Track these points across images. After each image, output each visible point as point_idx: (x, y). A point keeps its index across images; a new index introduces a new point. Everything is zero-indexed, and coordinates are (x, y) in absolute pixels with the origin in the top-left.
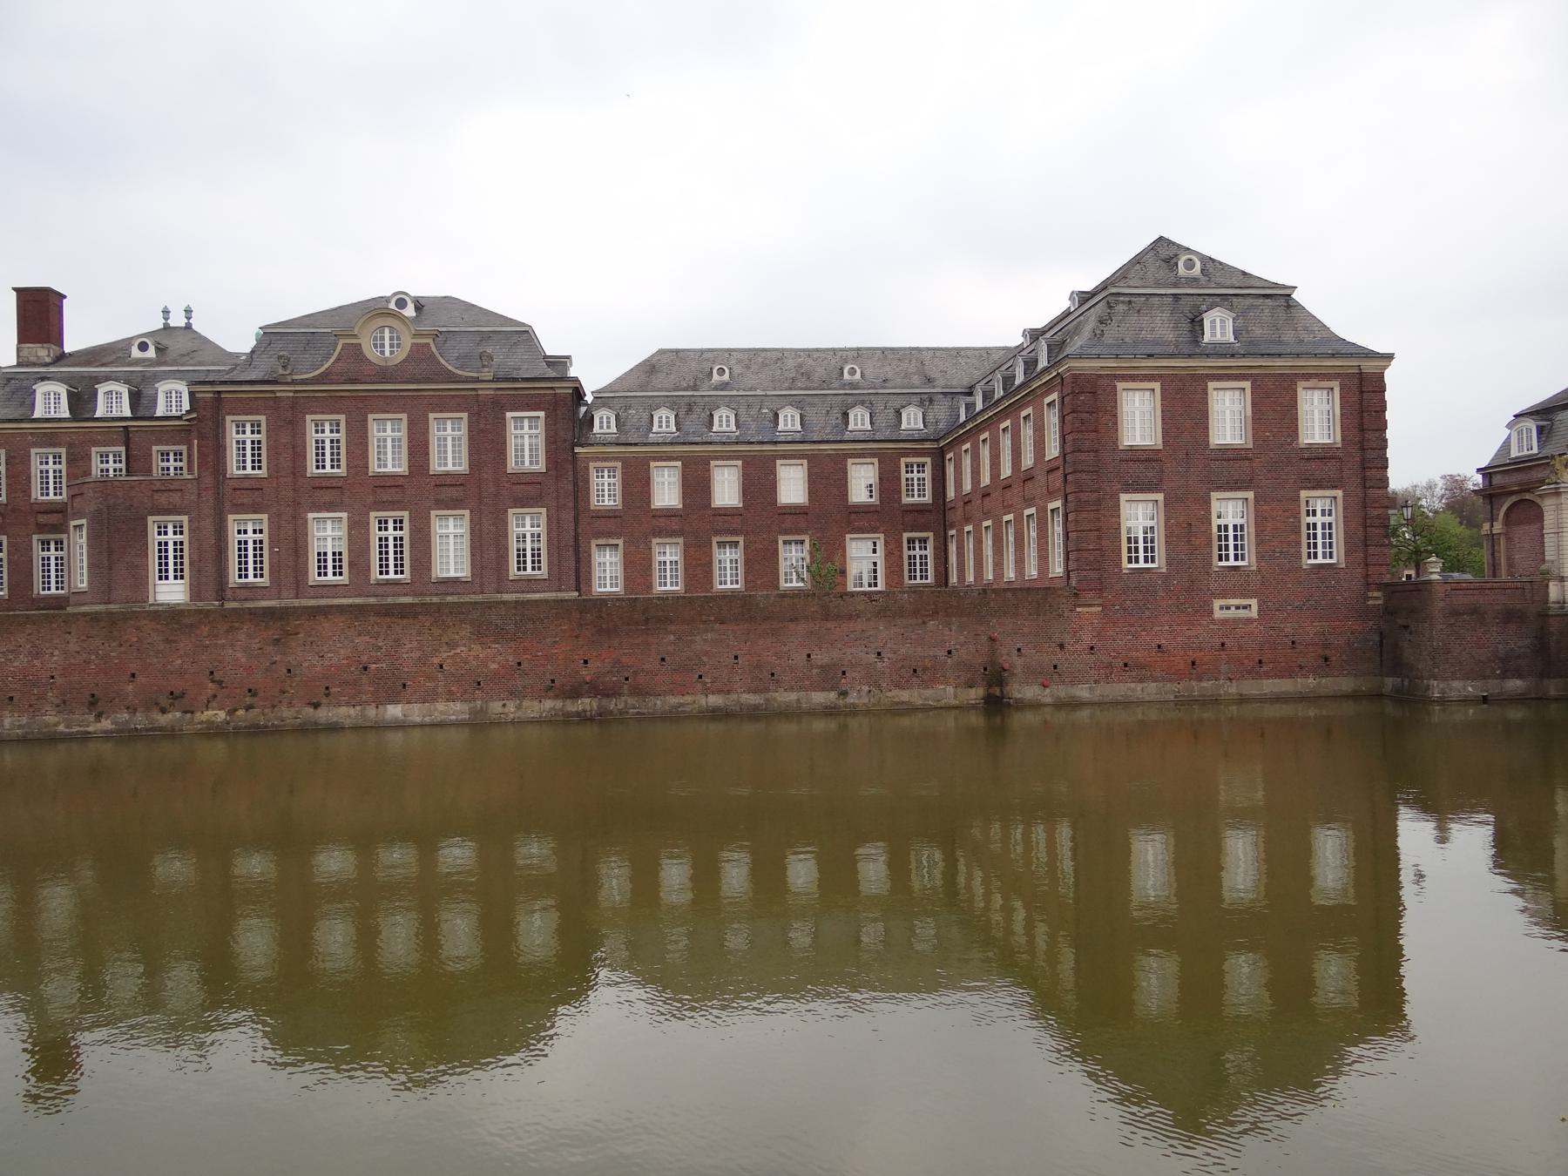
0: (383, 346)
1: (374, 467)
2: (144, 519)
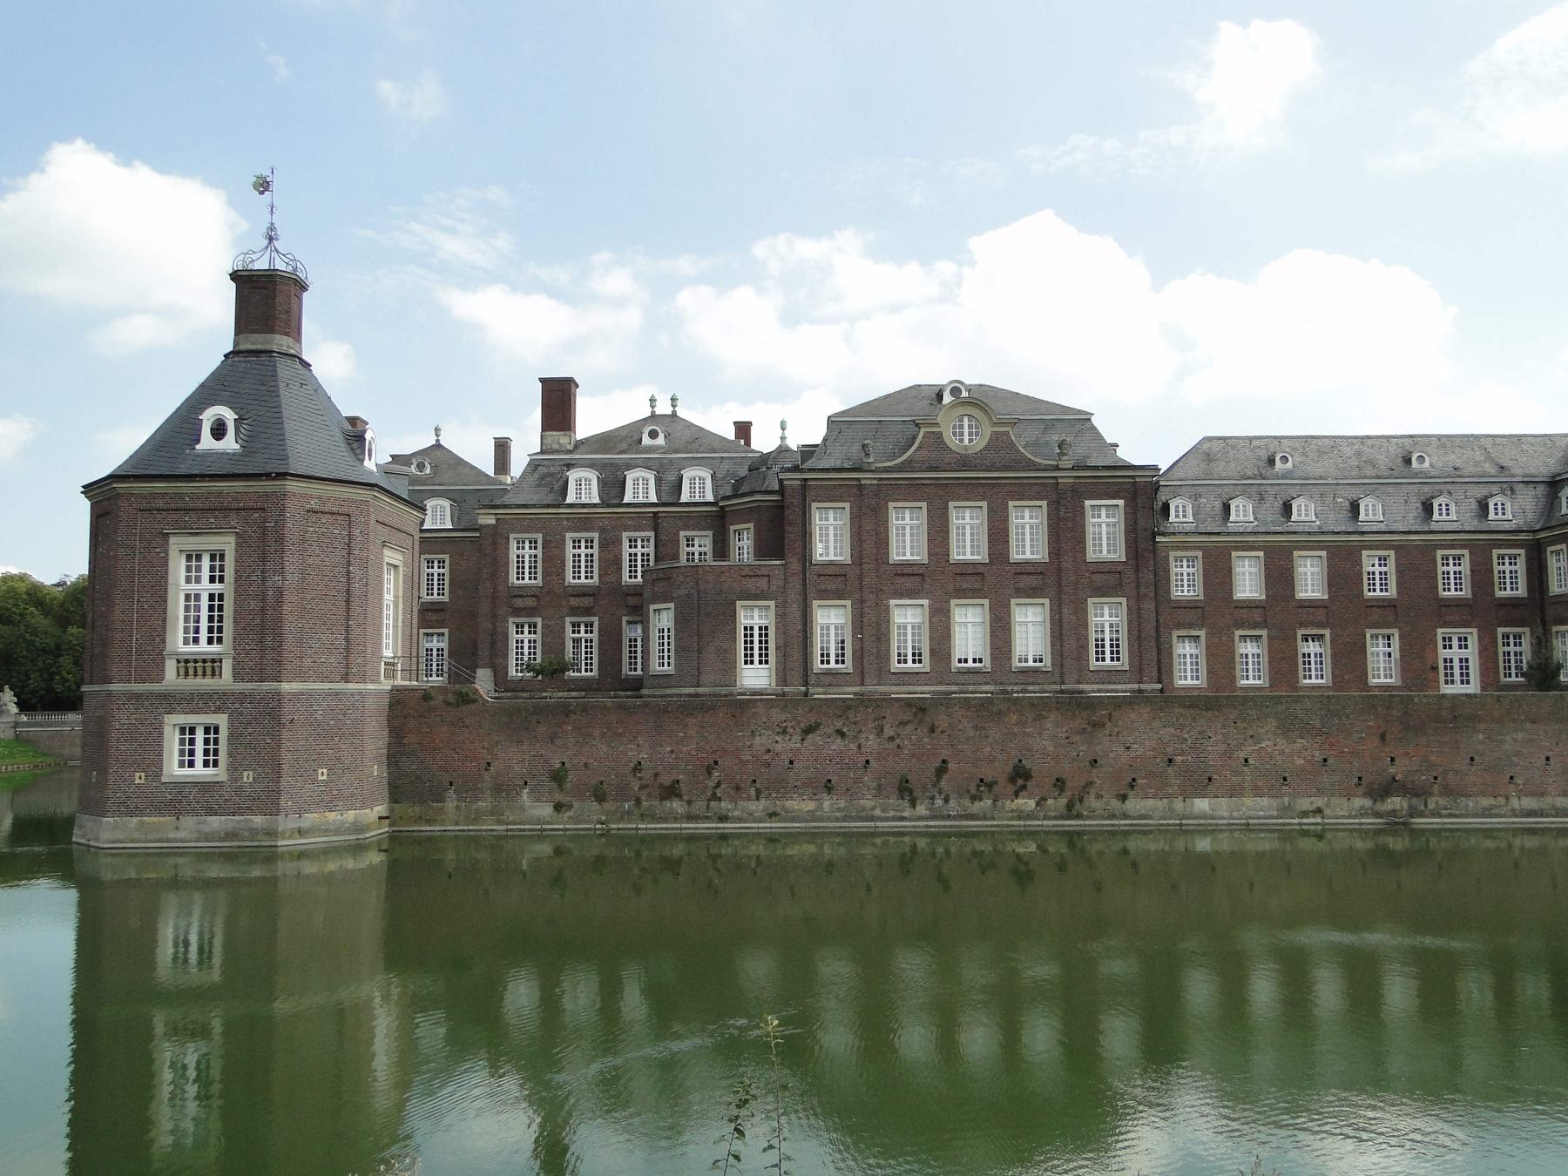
0: (962, 434)
1: (955, 556)
2: (733, 604)
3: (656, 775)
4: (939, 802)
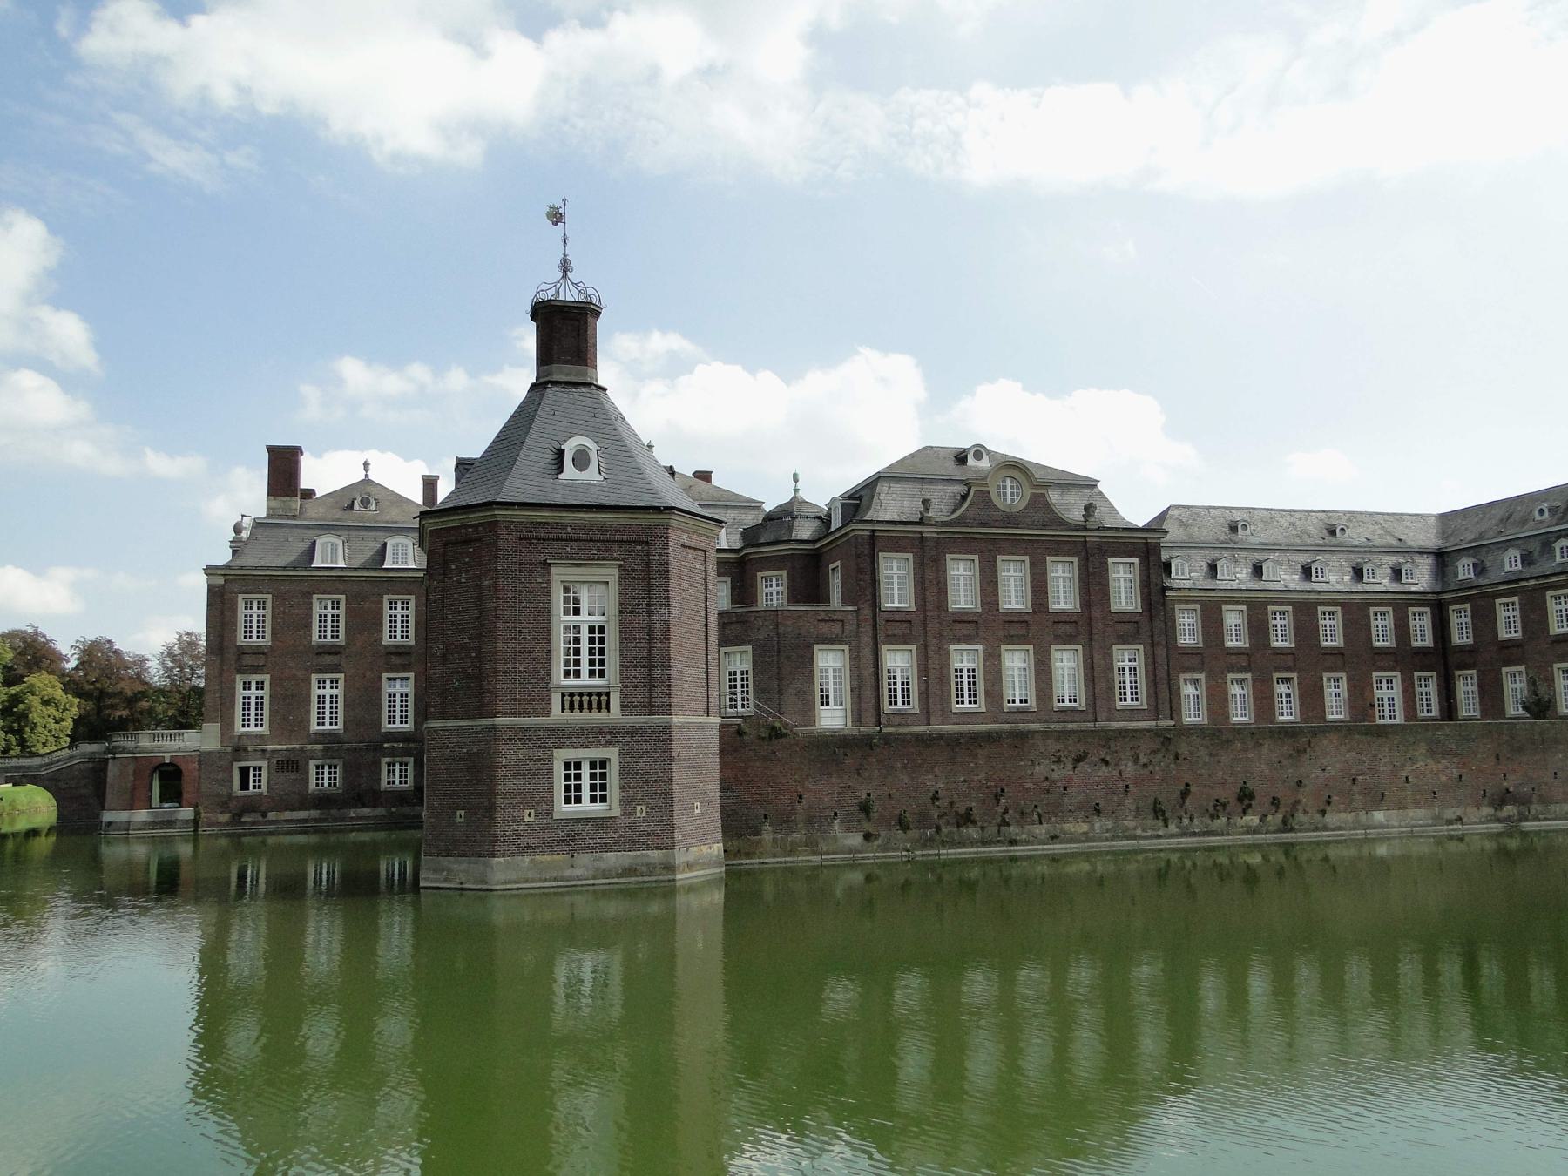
2: (810, 648)
3: (952, 803)
4: (1186, 821)
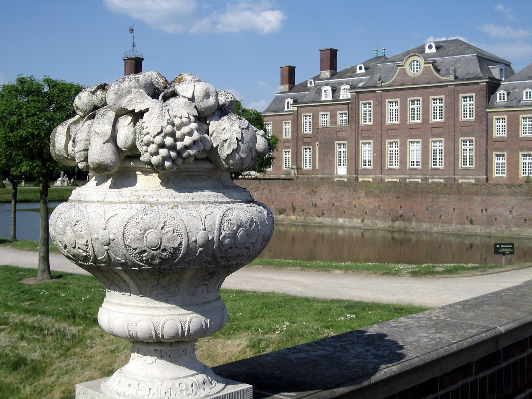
0: (414, 68)
2: (334, 142)
